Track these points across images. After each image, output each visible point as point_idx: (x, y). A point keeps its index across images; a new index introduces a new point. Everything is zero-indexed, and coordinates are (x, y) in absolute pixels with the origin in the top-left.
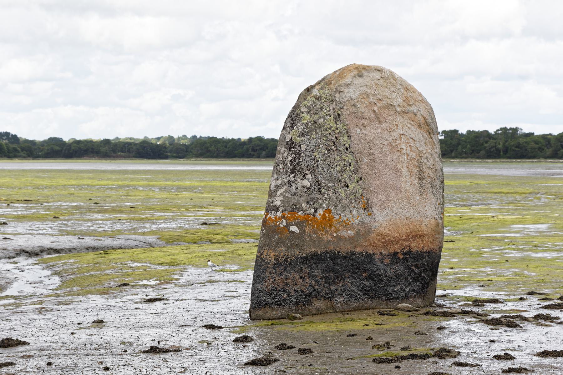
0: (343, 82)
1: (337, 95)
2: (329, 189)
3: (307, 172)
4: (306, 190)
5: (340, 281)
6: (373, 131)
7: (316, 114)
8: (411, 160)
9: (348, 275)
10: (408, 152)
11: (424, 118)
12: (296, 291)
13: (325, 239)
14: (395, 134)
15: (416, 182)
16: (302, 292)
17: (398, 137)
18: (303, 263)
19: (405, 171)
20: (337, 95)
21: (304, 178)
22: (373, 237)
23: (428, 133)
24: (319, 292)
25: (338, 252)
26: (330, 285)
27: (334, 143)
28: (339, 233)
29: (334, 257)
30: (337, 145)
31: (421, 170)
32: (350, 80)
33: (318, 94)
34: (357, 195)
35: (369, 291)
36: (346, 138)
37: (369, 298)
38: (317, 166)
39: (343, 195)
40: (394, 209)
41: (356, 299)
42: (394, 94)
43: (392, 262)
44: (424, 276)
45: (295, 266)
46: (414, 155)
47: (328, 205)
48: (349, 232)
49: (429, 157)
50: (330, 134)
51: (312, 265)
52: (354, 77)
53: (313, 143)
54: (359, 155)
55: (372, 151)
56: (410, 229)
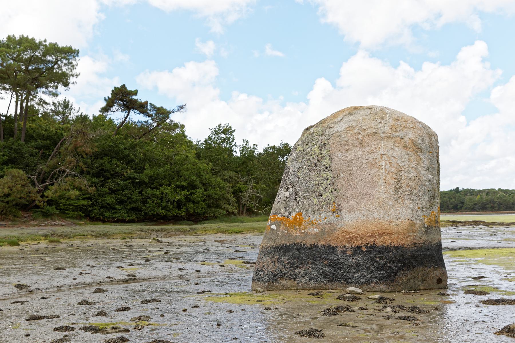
0: (333, 121)
1: (327, 130)
2: (304, 198)
3: (290, 186)
4: (285, 199)
6: (354, 154)
7: (306, 145)
8: (389, 174)
11: (412, 140)
12: (268, 272)
15: (391, 191)
16: (272, 272)
17: (379, 157)
19: (381, 182)
20: (327, 130)
21: (287, 190)
23: (413, 152)
24: (285, 274)
25: (304, 245)
26: (295, 269)
27: (316, 164)
28: (306, 230)
29: (300, 248)
30: (318, 165)
31: (398, 181)
32: (341, 118)
35: (329, 275)
36: (327, 160)
37: (328, 281)
38: (298, 181)
39: (315, 202)
41: (316, 281)
43: (355, 254)
44: (390, 267)
45: (270, 254)
47: (300, 210)
48: (315, 229)
49: (412, 170)
50: (313, 158)
52: (345, 115)
53: (299, 165)
54: (338, 172)
55: (350, 169)
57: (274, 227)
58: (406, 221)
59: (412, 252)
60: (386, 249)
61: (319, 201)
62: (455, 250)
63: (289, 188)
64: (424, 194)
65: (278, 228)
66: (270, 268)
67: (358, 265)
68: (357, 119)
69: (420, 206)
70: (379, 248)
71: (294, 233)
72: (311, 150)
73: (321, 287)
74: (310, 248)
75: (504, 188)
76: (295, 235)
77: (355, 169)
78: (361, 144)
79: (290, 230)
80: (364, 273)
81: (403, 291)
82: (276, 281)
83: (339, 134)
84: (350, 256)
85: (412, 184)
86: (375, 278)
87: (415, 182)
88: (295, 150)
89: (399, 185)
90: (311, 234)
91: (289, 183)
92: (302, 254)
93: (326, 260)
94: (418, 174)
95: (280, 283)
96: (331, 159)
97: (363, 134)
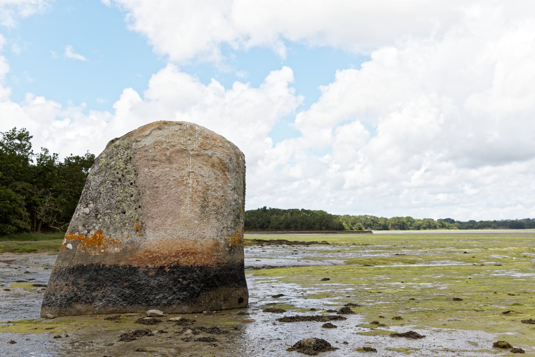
0: (140, 135)
1: (134, 144)
2: (105, 215)
3: (91, 202)
4: (84, 215)
5: (101, 289)
6: (162, 170)
7: (111, 158)
9: (109, 284)
10: (194, 185)
11: (220, 159)
12: (61, 296)
13: (93, 254)
14: (183, 172)
15: (197, 210)
16: (65, 296)
17: (187, 174)
18: (70, 273)
19: (187, 201)
20: (134, 144)
21: (87, 206)
22: (139, 253)
24: (80, 297)
25: (103, 265)
26: (92, 292)
27: (120, 180)
28: (106, 250)
29: (98, 269)
30: (122, 181)
31: (205, 200)
32: (149, 132)
33: (118, 144)
34: (132, 219)
35: (128, 298)
36: (132, 176)
37: (128, 304)
38: (100, 197)
39: (117, 220)
40: (168, 231)
41: (115, 304)
42: (189, 142)
43: (157, 274)
44: (193, 288)
45: (64, 275)
46: (200, 188)
48: (116, 249)
49: (218, 190)
50: (117, 173)
51: (77, 275)
52: (154, 130)
53: (101, 179)
55: (156, 185)
56: (182, 247)
57: (70, 246)
58: (211, 240)
59: (215, 272)
60: (189, 269)
61: (121, 219)
62: (259, 269)
63: (89, 204)
64: (229, 214)
65: (75, 247)
66: (63, 292)
67: (160, 286)
68: (165, 135)
69: (225, 225)
70: (183, 268)
71: (93, 253)
72: (115, 164)
73: (120, 310)
74: (110, 269)
75: (306, 209)
76: (93, 254)
77: (161, 186)
78: (169, 160)
79: (88, 249)
80: (166, 294)
81: (205, 312)
82: (70, 305)
83: (146, 148)
84: (152, 277)
85: (218, 203)
86: (177, 299)
87: (221, 201)
88: (98, 163)
89: (206, 203)
90: (112, 254)
91: (89, 199)
92: (101, 275)
93: (126, 281)
94: (224, 193)
95: (74, 308)
96: (137, 175)
97: (171, 150)
